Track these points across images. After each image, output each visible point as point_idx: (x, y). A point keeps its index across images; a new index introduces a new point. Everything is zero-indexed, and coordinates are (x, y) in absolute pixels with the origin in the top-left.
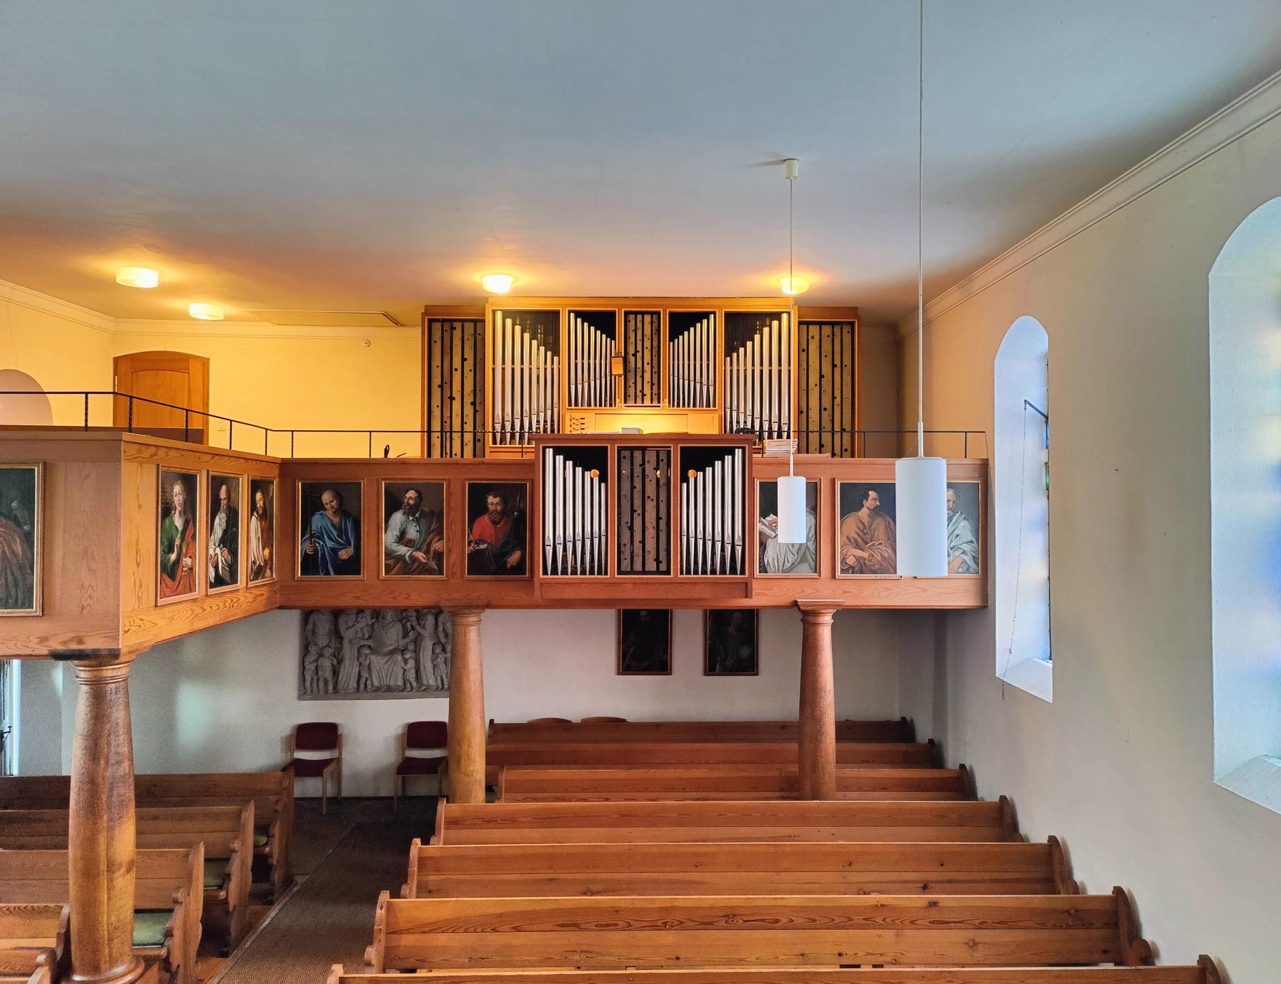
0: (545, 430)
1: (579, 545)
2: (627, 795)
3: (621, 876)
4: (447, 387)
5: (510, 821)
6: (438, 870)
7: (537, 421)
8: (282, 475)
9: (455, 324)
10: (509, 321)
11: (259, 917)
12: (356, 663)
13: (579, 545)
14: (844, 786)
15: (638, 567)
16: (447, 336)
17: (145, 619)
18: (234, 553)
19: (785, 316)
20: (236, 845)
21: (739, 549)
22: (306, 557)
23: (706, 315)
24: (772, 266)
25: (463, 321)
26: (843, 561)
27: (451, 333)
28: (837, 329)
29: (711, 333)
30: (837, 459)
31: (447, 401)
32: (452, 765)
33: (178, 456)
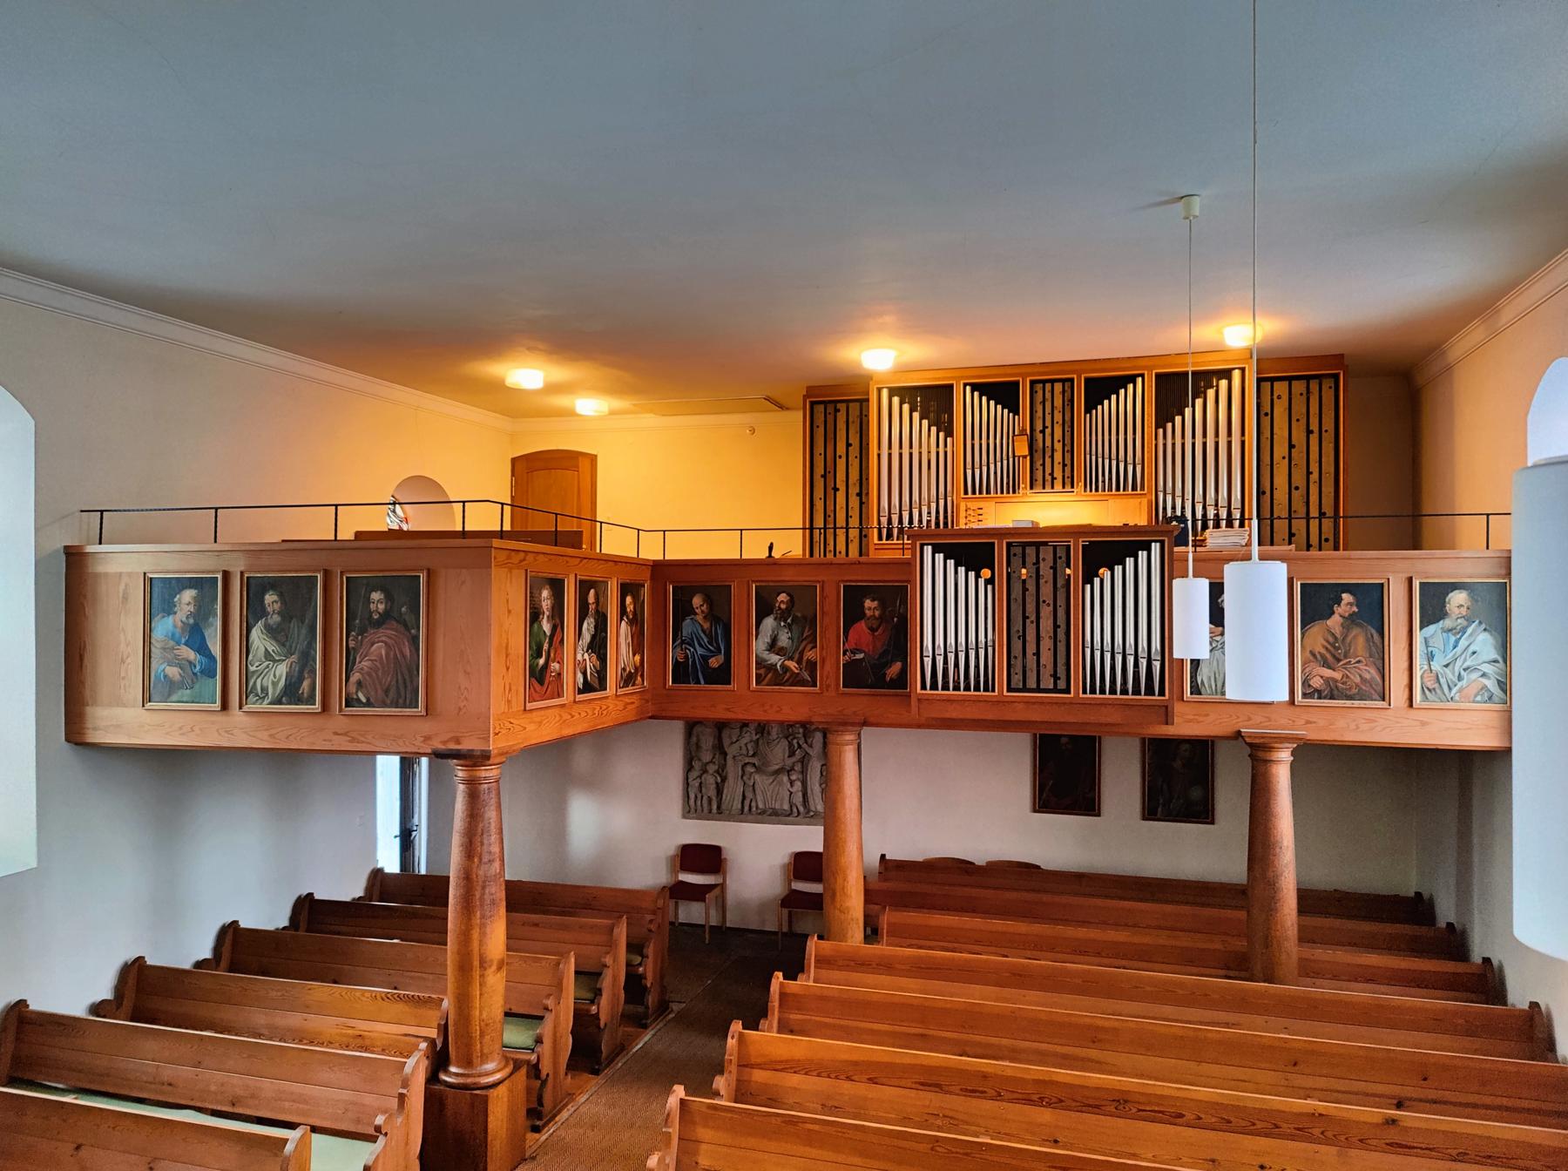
0: (937, 524)
1: (962, 656)
2: (1028, 953)
3: (1005, 1042)
4: (830, 477)
5: (886, 966)
6: (800, 1009)
7: (926, 515)
8: (653, 578)
10: (896, 400)
11: (634, 1038)
12: (740, 783)
13: (962, 656)
14: (1308, 971)
15: (1032, 683)
16: (830, 419)
17: (511, 719)
18: (603, 659)
19: (1236, 375)
20: (608, 960)
21: (1157, 665)
22: (676, 664)
23: (1132, 379)
24: (1215, 312)
26: (1305, 683)
27: (833, 416)
28: (1314, 385)
29: (1135, 401)
30: (1314, 553)
32: (827, 900)
33: (546, 559)
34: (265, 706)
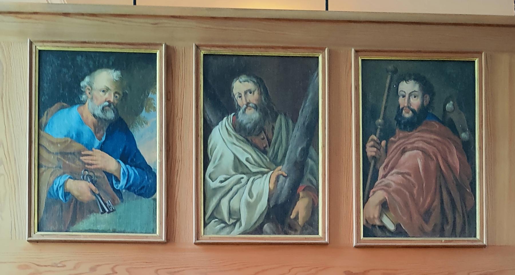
34: (235, 235)
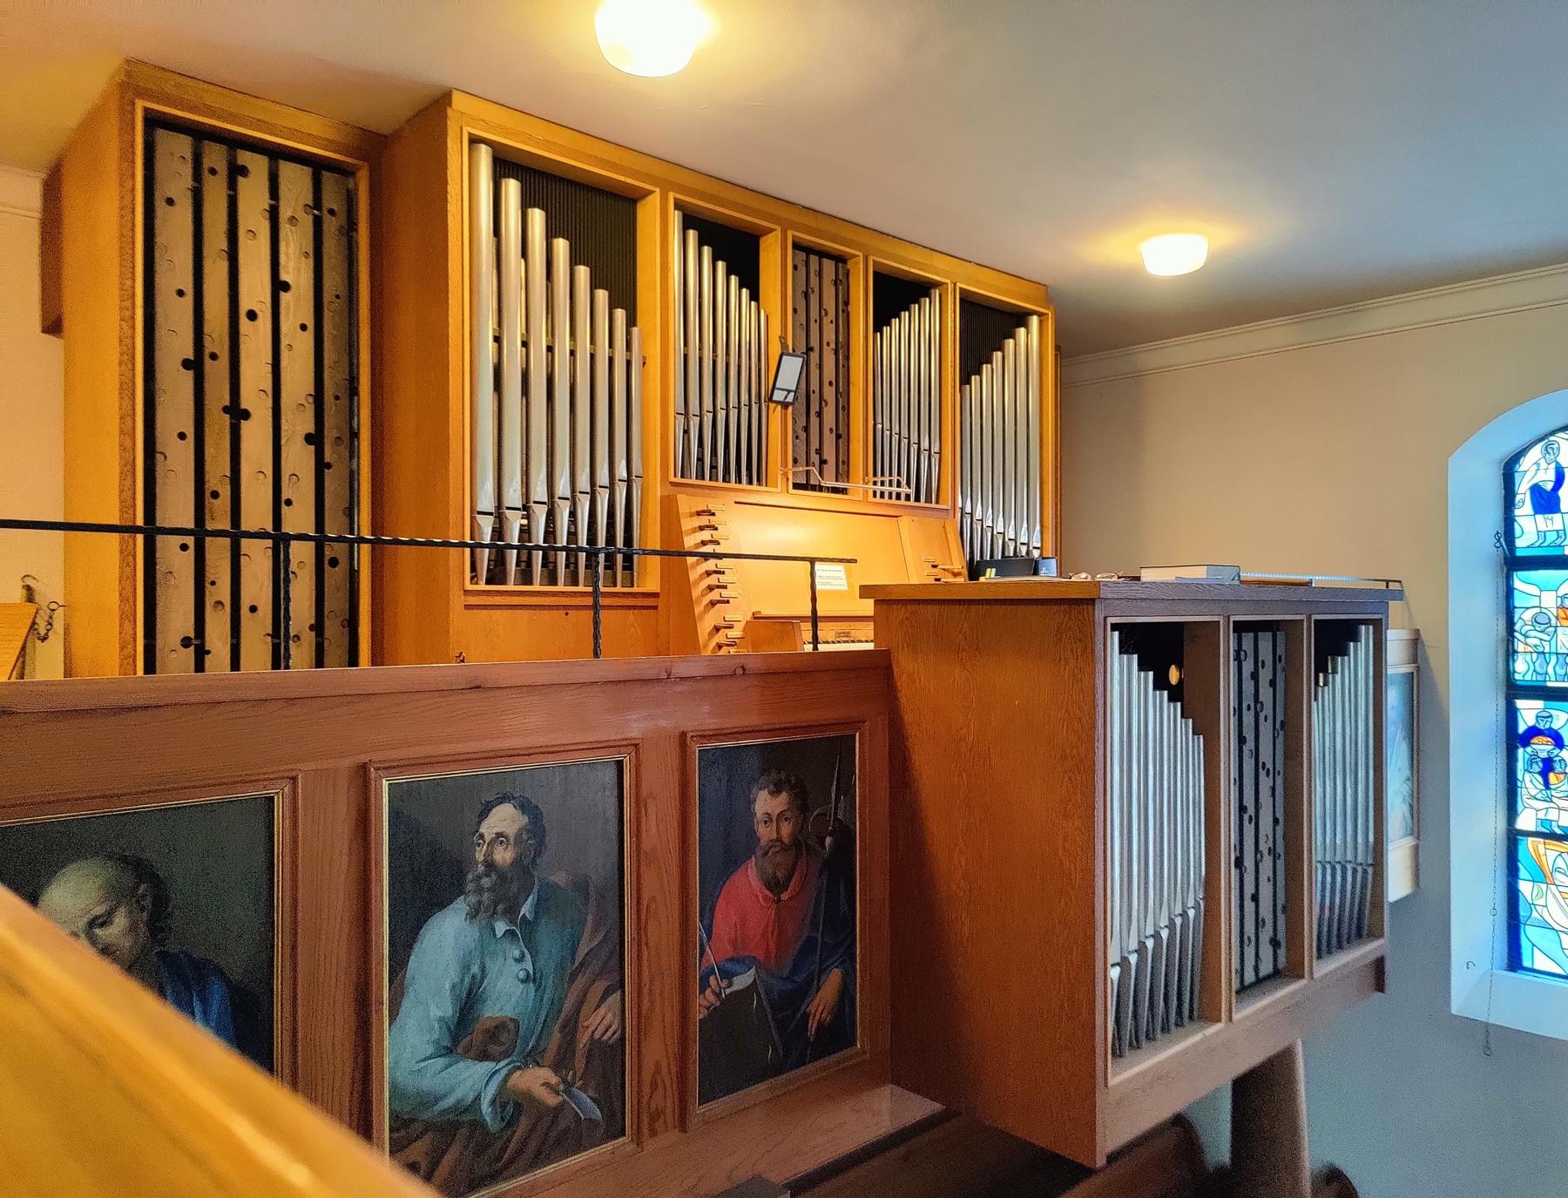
4: (217, 373)
9: (245, 158)
16: (215, 192)
25: (276, 154)
29: (929, 330)
31: (217, 423)
